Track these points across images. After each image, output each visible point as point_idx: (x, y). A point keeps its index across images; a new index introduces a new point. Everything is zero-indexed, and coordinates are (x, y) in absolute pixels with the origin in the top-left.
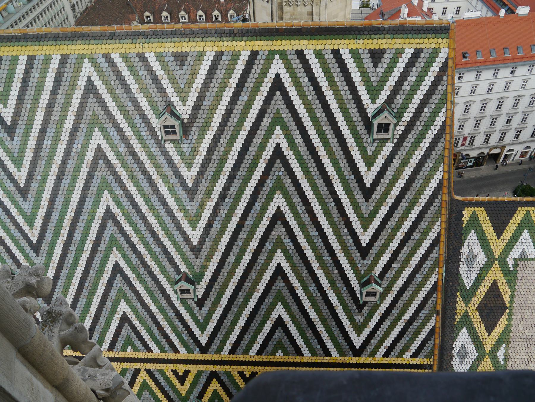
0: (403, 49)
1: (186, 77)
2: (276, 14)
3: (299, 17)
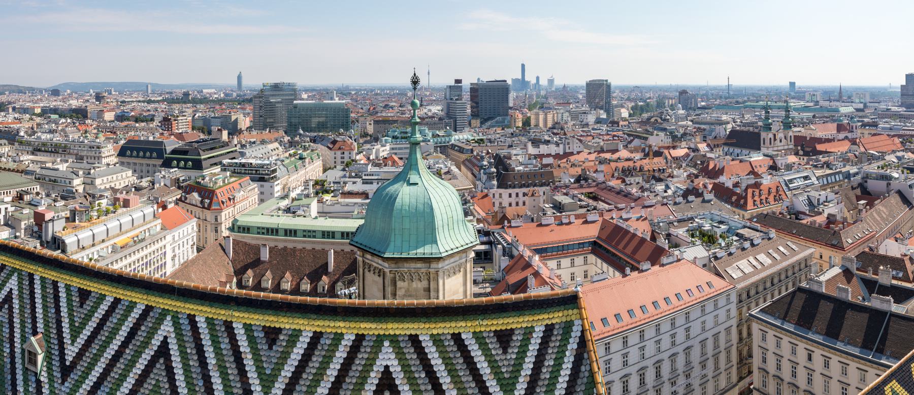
0: (532, 327)
1: (275, 361)
2: (389, 289)
3: (414, 293)
